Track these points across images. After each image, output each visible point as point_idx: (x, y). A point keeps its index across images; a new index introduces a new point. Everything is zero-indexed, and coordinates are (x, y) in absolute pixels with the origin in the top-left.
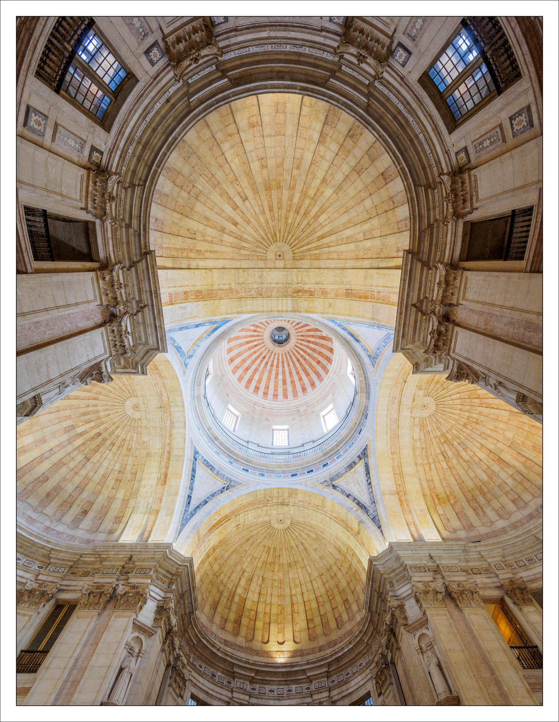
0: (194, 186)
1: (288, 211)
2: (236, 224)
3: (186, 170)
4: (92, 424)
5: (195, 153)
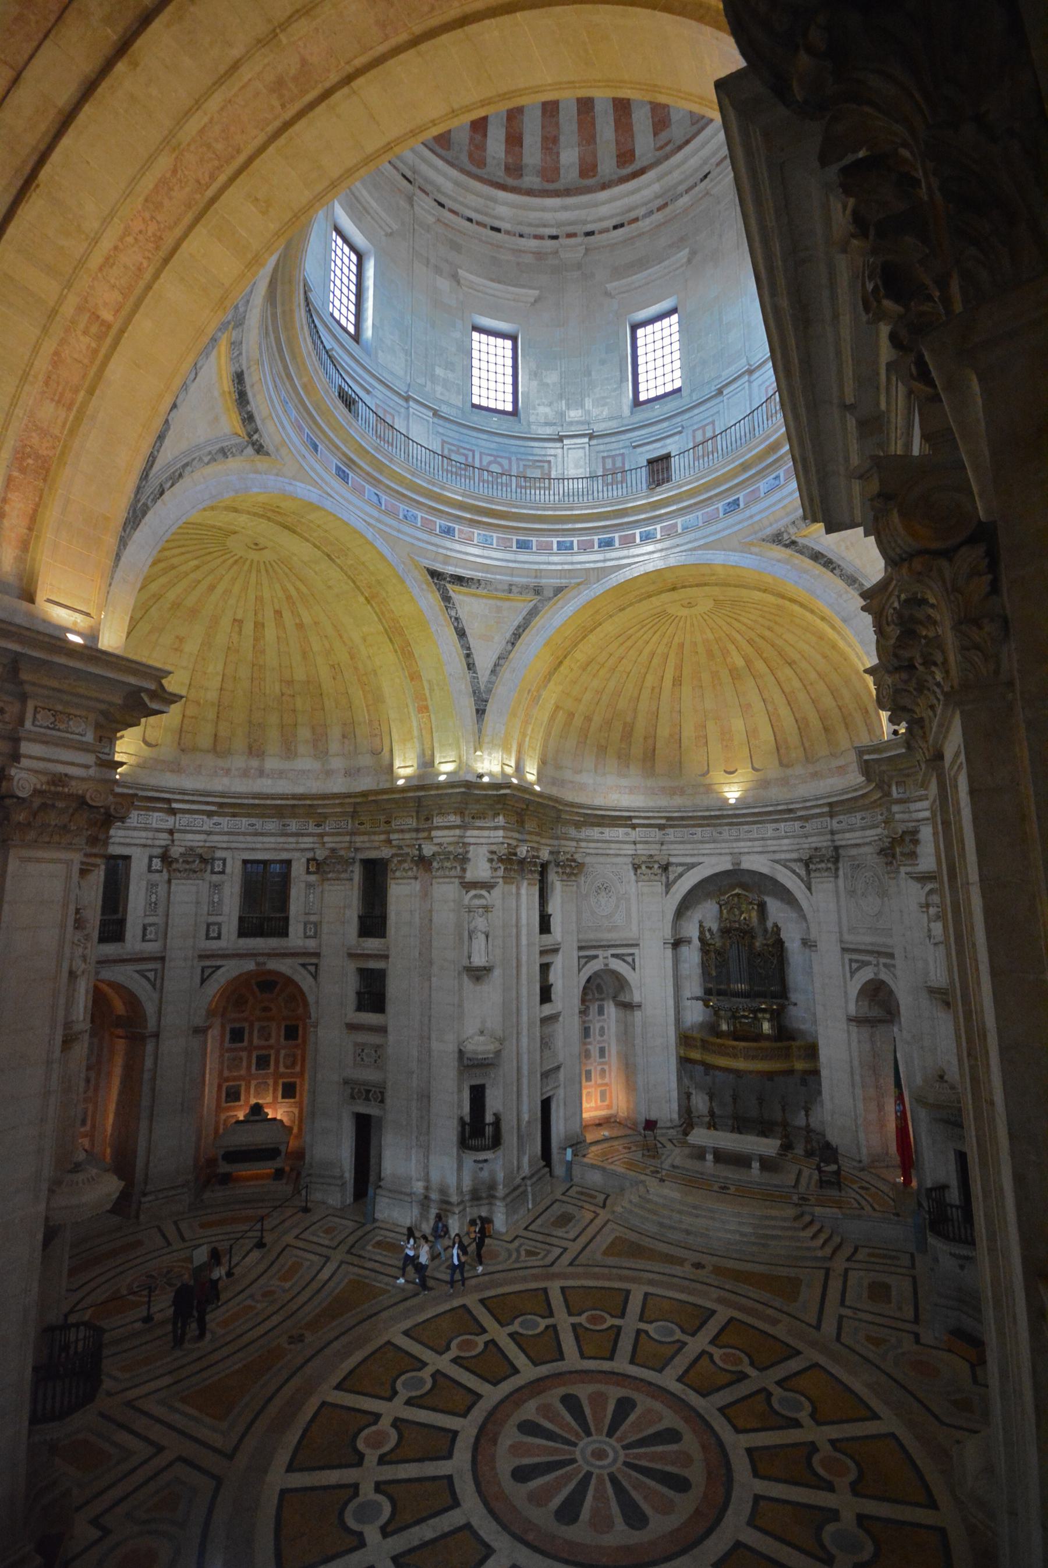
0: (282, 695)
1: (187, 574)
2: (278, 613)
3: (273, 719)
4: (731, 647)
5: (250, 722)
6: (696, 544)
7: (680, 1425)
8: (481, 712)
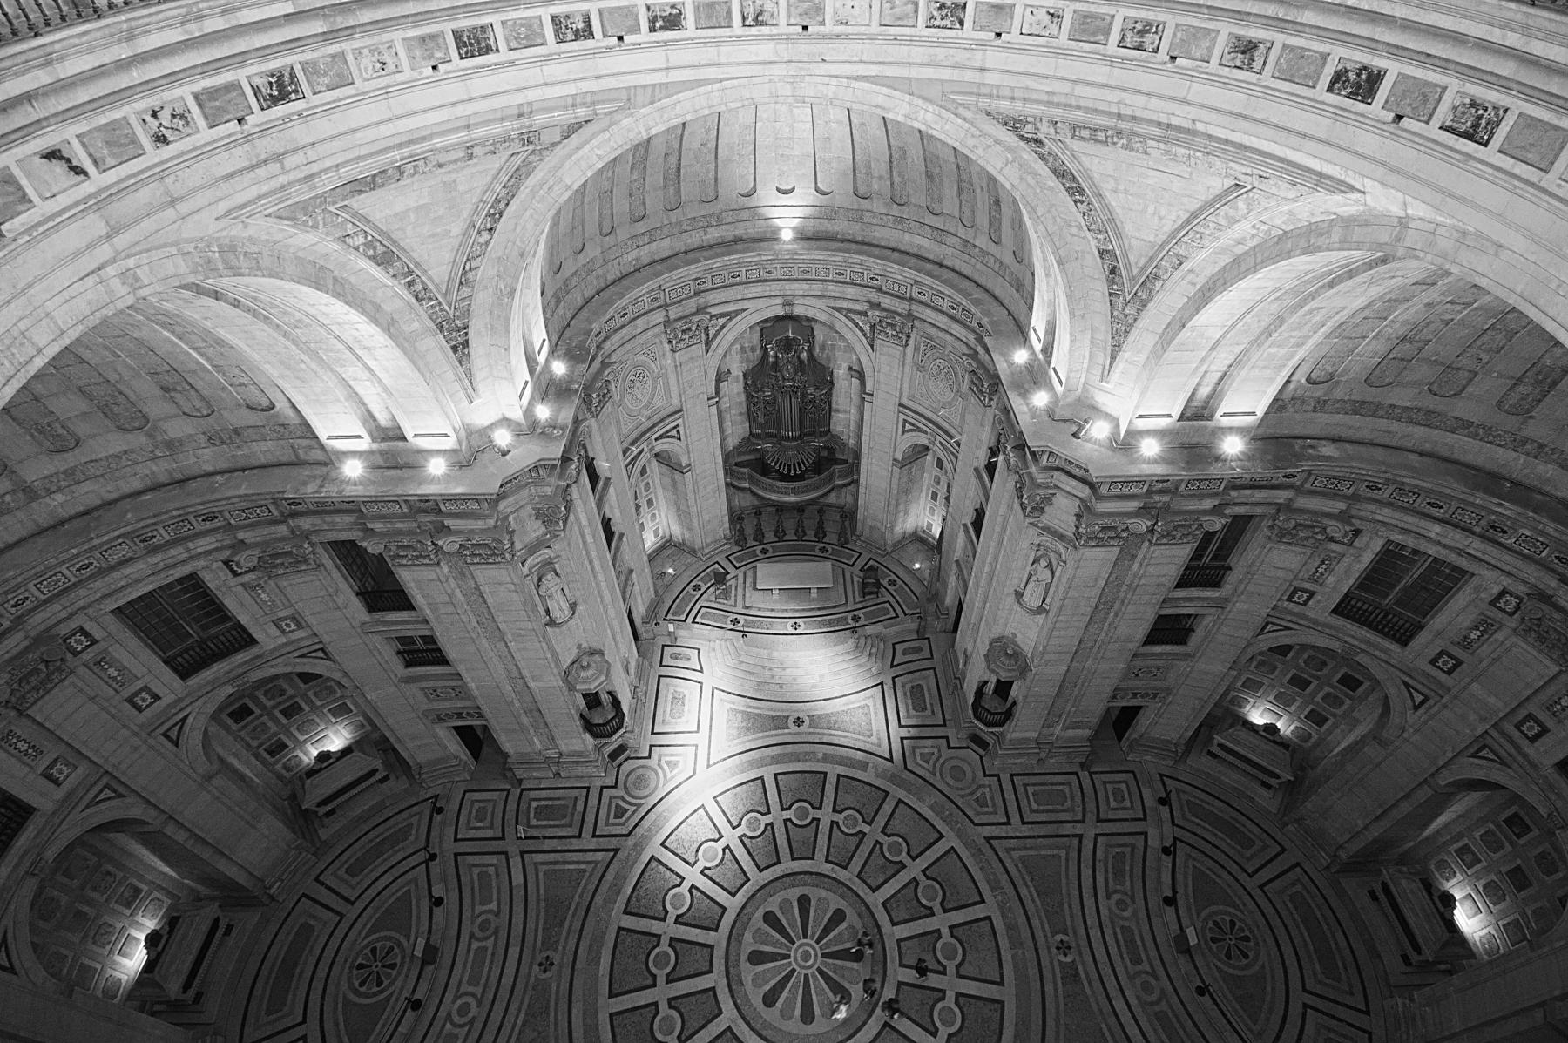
6: (862, 70)
7: (843, 904)
8: (461, 348)
